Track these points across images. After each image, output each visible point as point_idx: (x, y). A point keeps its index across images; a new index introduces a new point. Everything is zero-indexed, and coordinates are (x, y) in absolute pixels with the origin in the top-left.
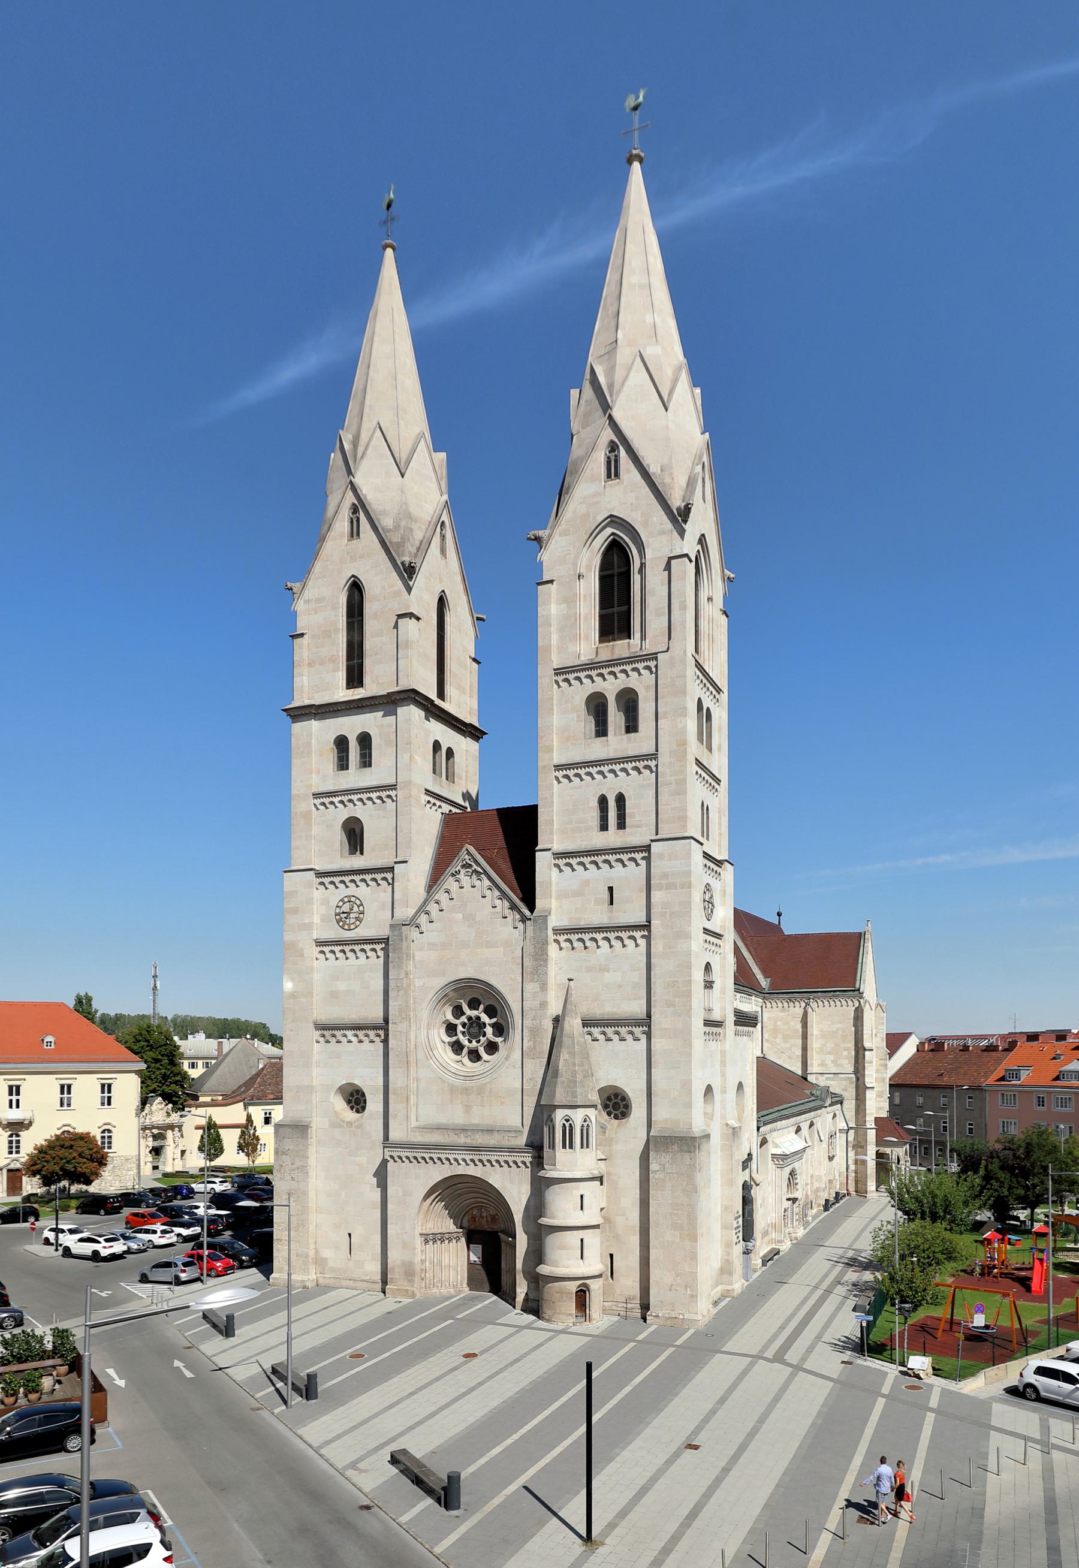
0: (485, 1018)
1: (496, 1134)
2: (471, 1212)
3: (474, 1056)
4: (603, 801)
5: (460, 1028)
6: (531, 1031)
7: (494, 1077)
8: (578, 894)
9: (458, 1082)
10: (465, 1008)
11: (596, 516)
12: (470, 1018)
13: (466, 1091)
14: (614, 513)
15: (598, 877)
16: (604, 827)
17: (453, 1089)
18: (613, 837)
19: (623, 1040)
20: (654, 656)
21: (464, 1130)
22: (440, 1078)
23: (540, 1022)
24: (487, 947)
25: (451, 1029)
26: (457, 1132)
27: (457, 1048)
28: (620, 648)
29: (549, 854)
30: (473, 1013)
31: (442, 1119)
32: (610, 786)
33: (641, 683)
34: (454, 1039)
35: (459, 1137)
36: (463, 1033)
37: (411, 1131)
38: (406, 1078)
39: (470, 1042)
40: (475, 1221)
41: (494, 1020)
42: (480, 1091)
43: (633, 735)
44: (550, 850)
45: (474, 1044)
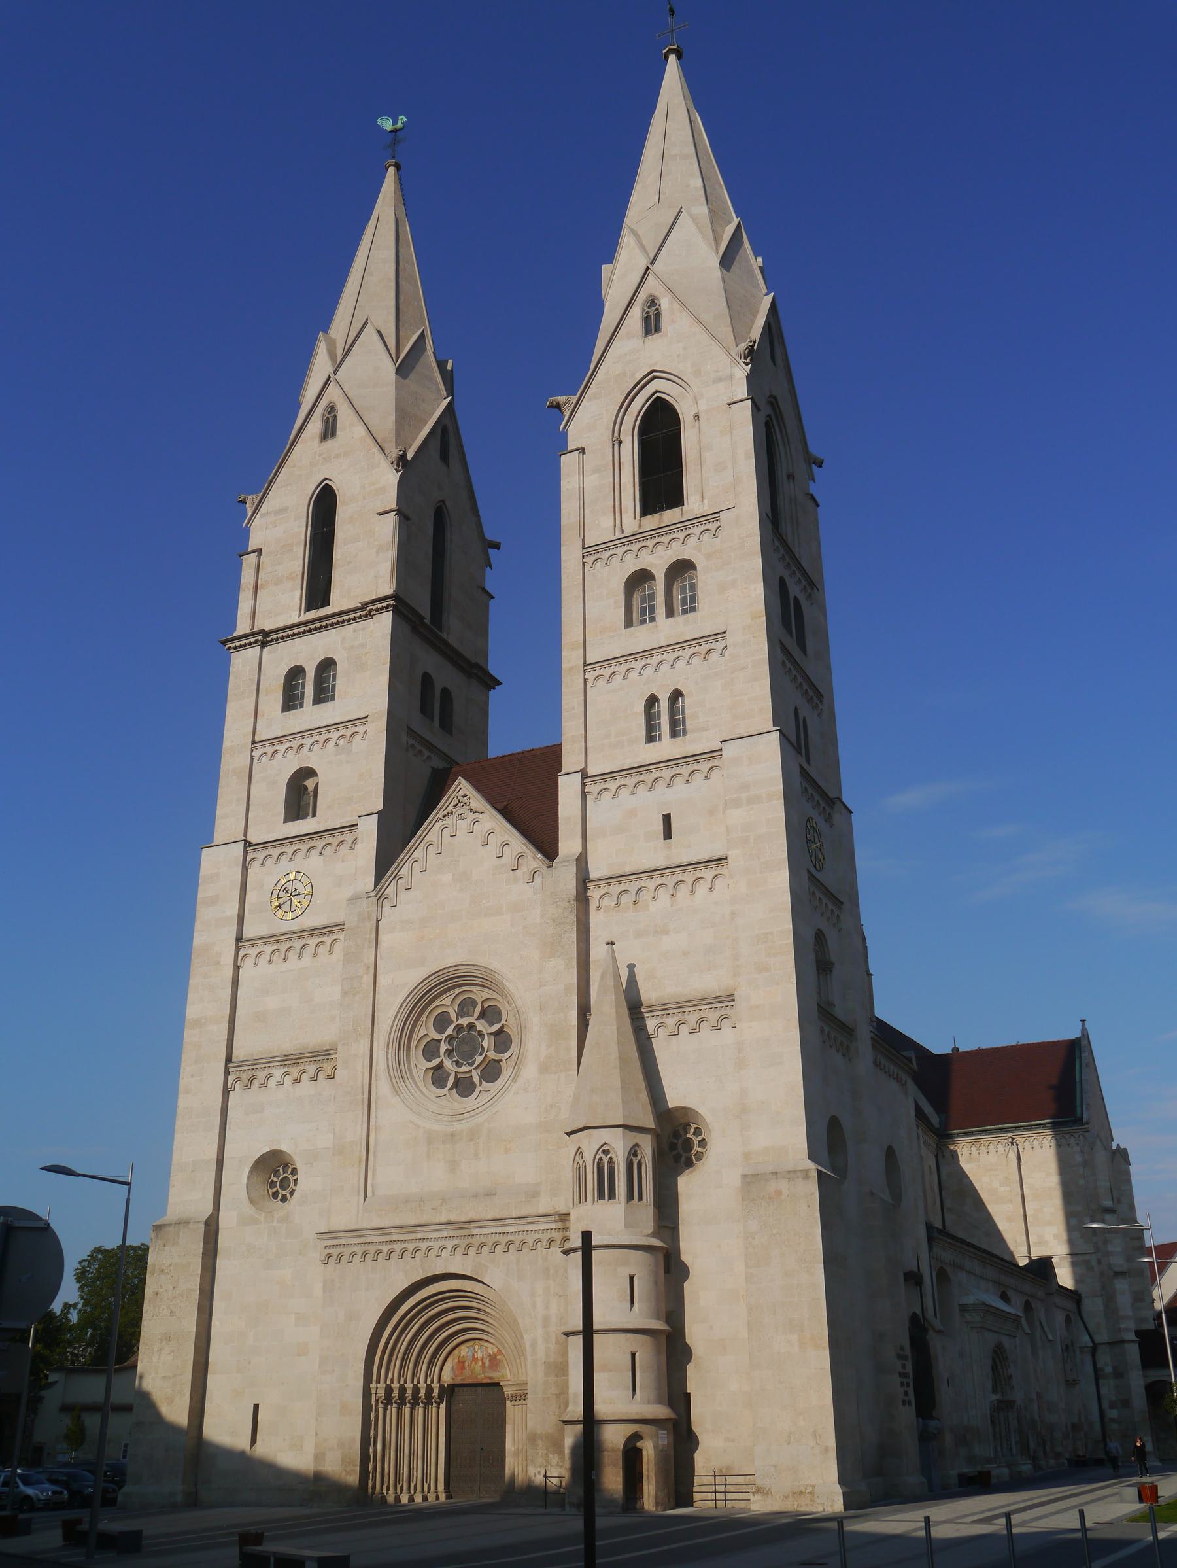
0: (481, 1026)
2: (456, 1352)
3: (464, 1087)
5: (443, 1047)
9: (440, 1127)
10: (453, 1016)
11: (634, 374)
12: (459, 1028)
16: (651, 736)
18: (667, 747)
22: (411, 1122)
25: (431, 1051)
27: (438, 1077)
28: (670, 516)
30: (464, 1021)
34: (436, 1062)
36: (449, 1053)
39: (458, 1064)
40: (463, 1368)
41: (496, 1028)
42: (473, 1135)
43: (690, 615)
45: (465, 1069)
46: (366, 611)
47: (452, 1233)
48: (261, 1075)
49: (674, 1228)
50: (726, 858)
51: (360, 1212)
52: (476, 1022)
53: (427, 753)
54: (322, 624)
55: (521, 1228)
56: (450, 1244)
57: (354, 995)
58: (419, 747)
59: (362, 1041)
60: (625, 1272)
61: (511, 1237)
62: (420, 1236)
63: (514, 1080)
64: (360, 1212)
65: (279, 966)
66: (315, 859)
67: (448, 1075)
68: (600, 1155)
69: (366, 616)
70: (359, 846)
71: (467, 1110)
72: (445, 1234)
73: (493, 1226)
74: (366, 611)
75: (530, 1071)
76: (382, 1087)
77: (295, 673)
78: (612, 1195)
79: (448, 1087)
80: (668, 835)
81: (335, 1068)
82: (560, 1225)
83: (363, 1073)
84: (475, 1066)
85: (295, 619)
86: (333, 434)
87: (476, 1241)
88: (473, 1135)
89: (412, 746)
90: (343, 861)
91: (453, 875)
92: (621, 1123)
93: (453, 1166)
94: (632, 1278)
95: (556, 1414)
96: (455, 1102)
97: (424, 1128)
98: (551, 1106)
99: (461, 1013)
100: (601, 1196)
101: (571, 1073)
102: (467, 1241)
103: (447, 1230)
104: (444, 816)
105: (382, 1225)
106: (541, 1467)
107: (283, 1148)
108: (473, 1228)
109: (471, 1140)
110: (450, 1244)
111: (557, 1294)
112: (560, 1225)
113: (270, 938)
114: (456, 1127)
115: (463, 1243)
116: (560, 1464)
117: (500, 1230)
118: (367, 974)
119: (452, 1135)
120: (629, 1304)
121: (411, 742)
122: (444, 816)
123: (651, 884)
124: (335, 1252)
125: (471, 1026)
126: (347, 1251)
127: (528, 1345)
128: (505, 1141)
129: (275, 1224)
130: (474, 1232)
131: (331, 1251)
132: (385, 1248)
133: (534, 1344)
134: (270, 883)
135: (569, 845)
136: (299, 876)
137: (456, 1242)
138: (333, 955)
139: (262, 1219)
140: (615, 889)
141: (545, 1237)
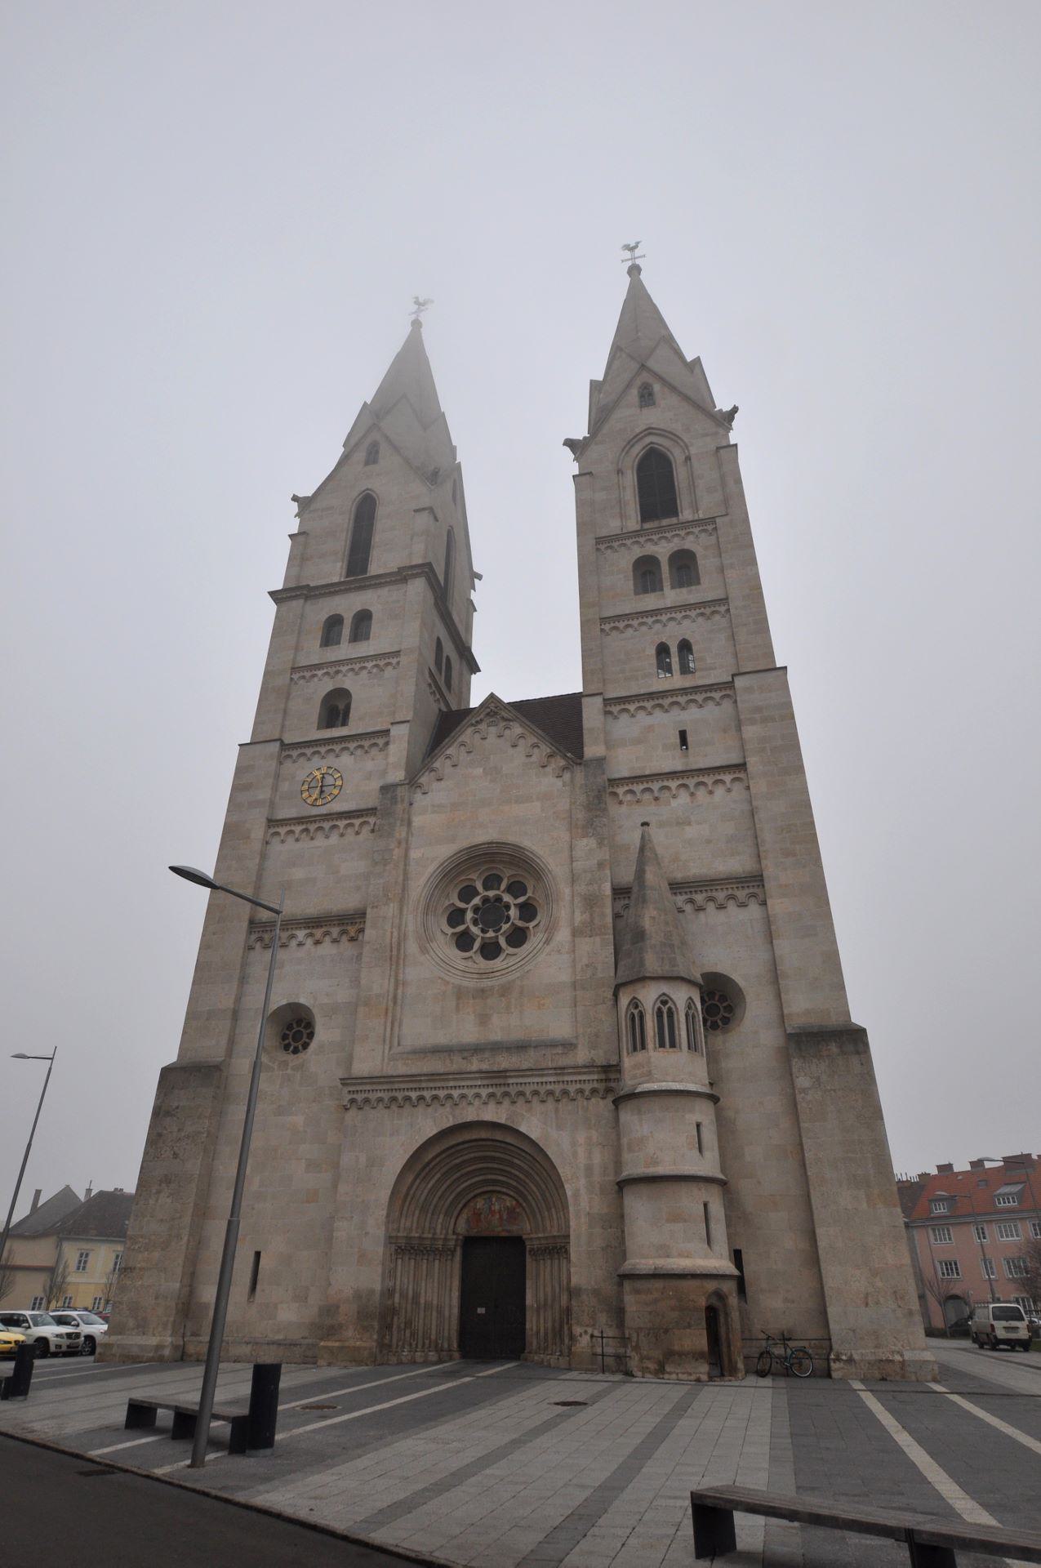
1: (532, 1052)
6: (585, 899)
7: (526, 969)
8: (638, 741)
9: (470, 983)
13: (482, 993)
14: (653, 426)
15: (666, 722)
17: (460, 993)
19: (721, 907)
20: (712, 520)
21: (476, 1049)
23: (600, 886)
24: (516, 802)
26: (466, 1054)
29: (599, 700)
31: (442, 1038)
32: (672, 635)
33: (699, 544)
35: (472, 1064)
37: (390, 1060)
38: (387, 981)
42: (505, 991)
44: (601, 694)
46: (402, 576)
47: (486, 1082)
51: (386, 1060)
52: (503, 895)
54: (362, 587)
55: (560, 1078)
56: (484, 1092)
57: (385, 865)
59: (392, 905)
61: (549, 1087)
62: (452, 1084)
63: (547, 942)
64: (386, 1060)
65: (305, 844)
66: (346, 760)
67: (474, 940)
69: (401, 580)
70: (391, 747)
71: (495, 970)
72: (479, 1083)
73: (532, 1075)
74: (402, 576)
75: (563, 935)
77: (334, 622)
79: (474, 950)
81: (362, 931)
82: (603, 1077)
83: (392, 933)
84: (502, 931)
85: (336, 579)
86: (375, 462)
87: (513, 1090)
88: (505, 991)
90: (373, 759)
91: (484, 769)
93: (483, 1020)
95: (604, 1268)
96: (483, 964)
97: (453, 984)
98: (587, 966)
101: (607, 937)
102: (503, 1089)
103: (481, 1078)
105: (409, 1073)
106: (587, 1326)
107: (302, 1001)
109: (503, 995)
110: (484, 1092)
111: (600, 1144)
112: (603, 1077)
113: (299, 820)
114: (486, 983)
115: (499, 1091)
116: (610, 1323)
117: (536, 1080)
118: (398, 847)
119: (483, 991)
123: (673, 784)
125: (499, 899)
126: (373, 1096)
127: (569, 1193)
128: (538, 997)
129: (289, 1071)
131: (355, 1096)
132: (414, 1095)
133: (576, 1195)
134: (302, 775)
136: (331, 771)
137: (490, 1090)
138: (361, 836)
139: (276, 1067)
140: (638, 788)
141: (587, 1087)
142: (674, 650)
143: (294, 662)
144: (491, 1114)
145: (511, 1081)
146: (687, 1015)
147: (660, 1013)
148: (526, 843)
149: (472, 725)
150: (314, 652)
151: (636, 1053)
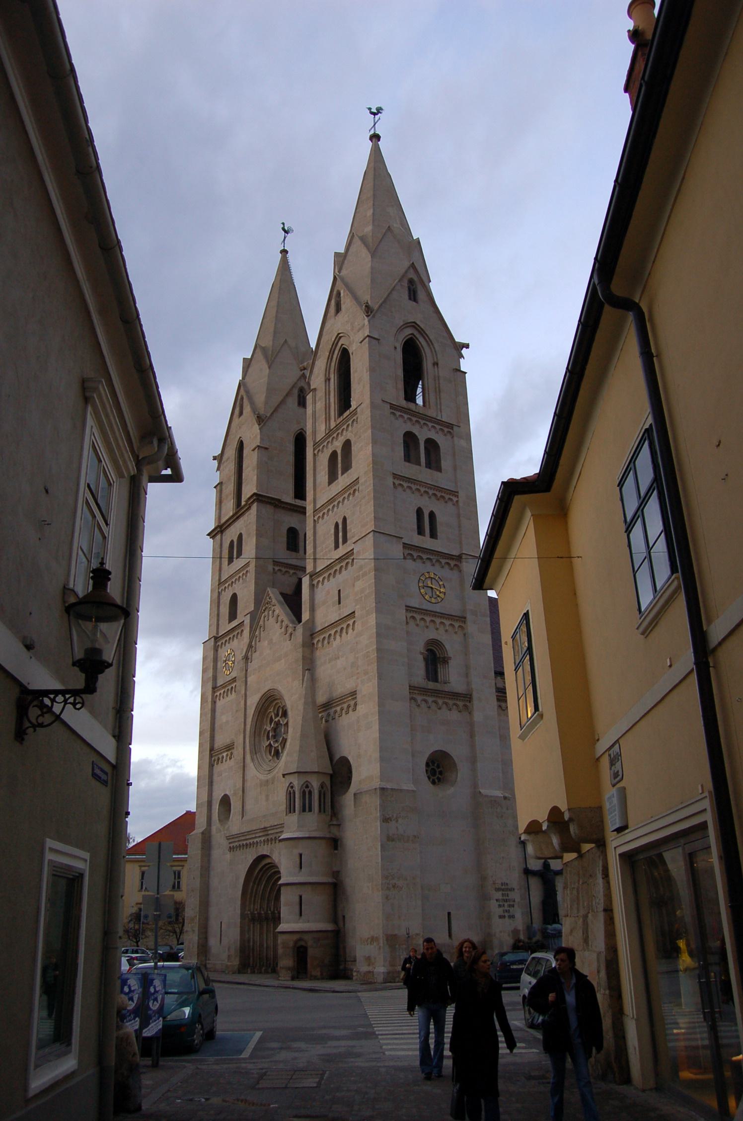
4: (337, 525)
9: (263, 777)
48: (220, 756)
49: (339, 825)
50: (354, 612)
53: (292, 571)
56: (262, 839)
58: (284, 570)
60: (296, 852)
68: (290, 789)
76: (248, 757)
78: (294, 811)
80: (339, 603)
89: (280, 570)
92: (295, 771)
94: (301, 855)
99: (277, 715)
100: (290, 812)
104: (264, 610)
108: (270, 830)
120: (298, 869)
121: (277, 568)
122: (264, 610)
124: (231, 845)
125: (279, 720)
130: (270, 832)
135: (305, 616)
142: (340, 526)
143: (220, 580)
144: (264, 850)
145: (270, 832)
146: (320, 792)
147: (304, 793)
148: (280, 688)
149: (263, 613)
150: (228, 570)
151: (304, 813)
